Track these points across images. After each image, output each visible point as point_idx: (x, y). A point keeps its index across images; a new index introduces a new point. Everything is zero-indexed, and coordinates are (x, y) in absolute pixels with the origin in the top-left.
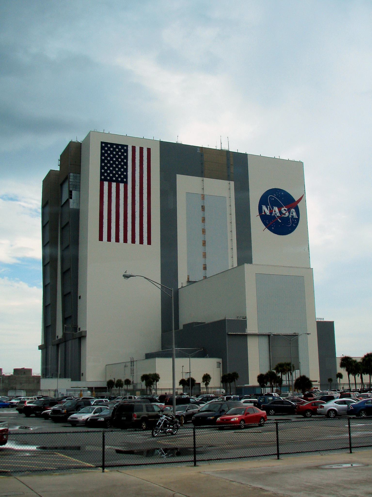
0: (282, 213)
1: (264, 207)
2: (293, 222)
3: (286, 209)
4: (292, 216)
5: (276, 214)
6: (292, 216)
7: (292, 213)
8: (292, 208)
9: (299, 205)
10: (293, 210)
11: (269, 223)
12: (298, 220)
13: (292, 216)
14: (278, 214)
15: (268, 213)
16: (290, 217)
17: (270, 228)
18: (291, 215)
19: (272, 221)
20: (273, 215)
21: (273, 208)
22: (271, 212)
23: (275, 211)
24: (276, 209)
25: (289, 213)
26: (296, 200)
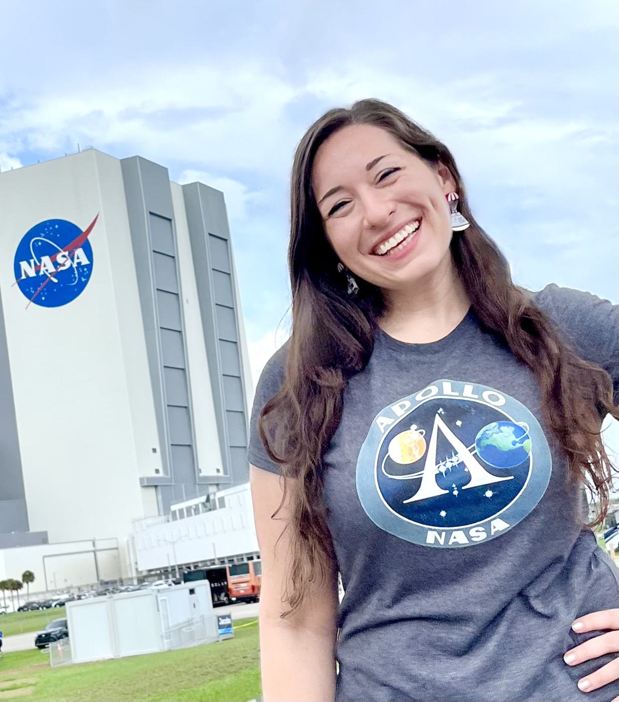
0: (60, 264)
1: (24, 265)
2: (81, 275)
3: (66, 253)
4: (79, 264)
5: (47, 270)
6: (78, 263)
7: (78, 258)
8: (76, 247)
9: (90, 237)
10: (80, 252)
11: (35, 290)
12: (90, 267)
13: (78, 263)
14: (52, 269)
15: (32, 273)
16: (75, 265)
17: (38, 301)
18: (76, 261)
19: (39, 286)
20: (41, 273)
21: (40, 261)
22: (37, 271)
23: (45, 266)
24: (46, 260)
25: (73, 259)
26: (84, 229)
